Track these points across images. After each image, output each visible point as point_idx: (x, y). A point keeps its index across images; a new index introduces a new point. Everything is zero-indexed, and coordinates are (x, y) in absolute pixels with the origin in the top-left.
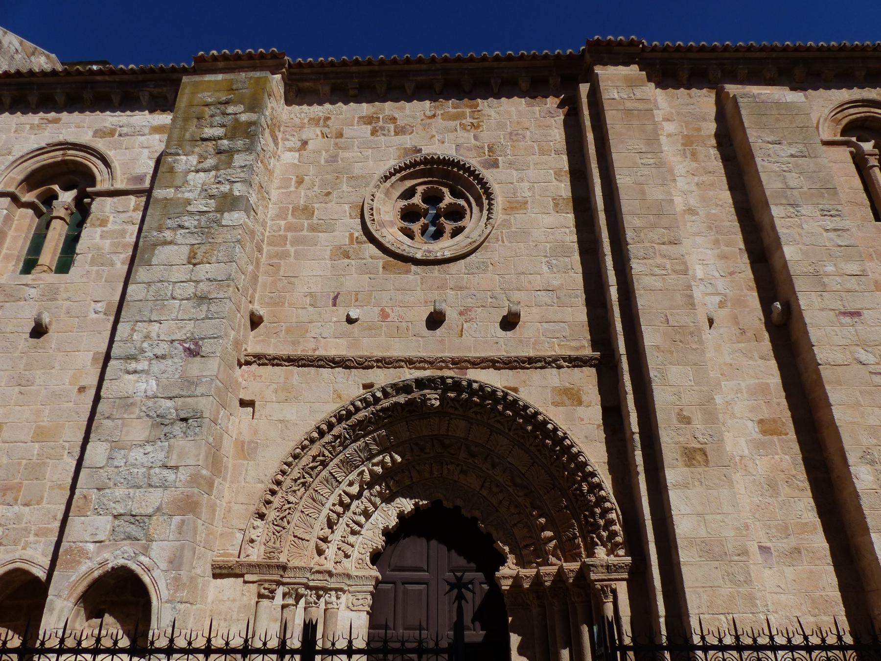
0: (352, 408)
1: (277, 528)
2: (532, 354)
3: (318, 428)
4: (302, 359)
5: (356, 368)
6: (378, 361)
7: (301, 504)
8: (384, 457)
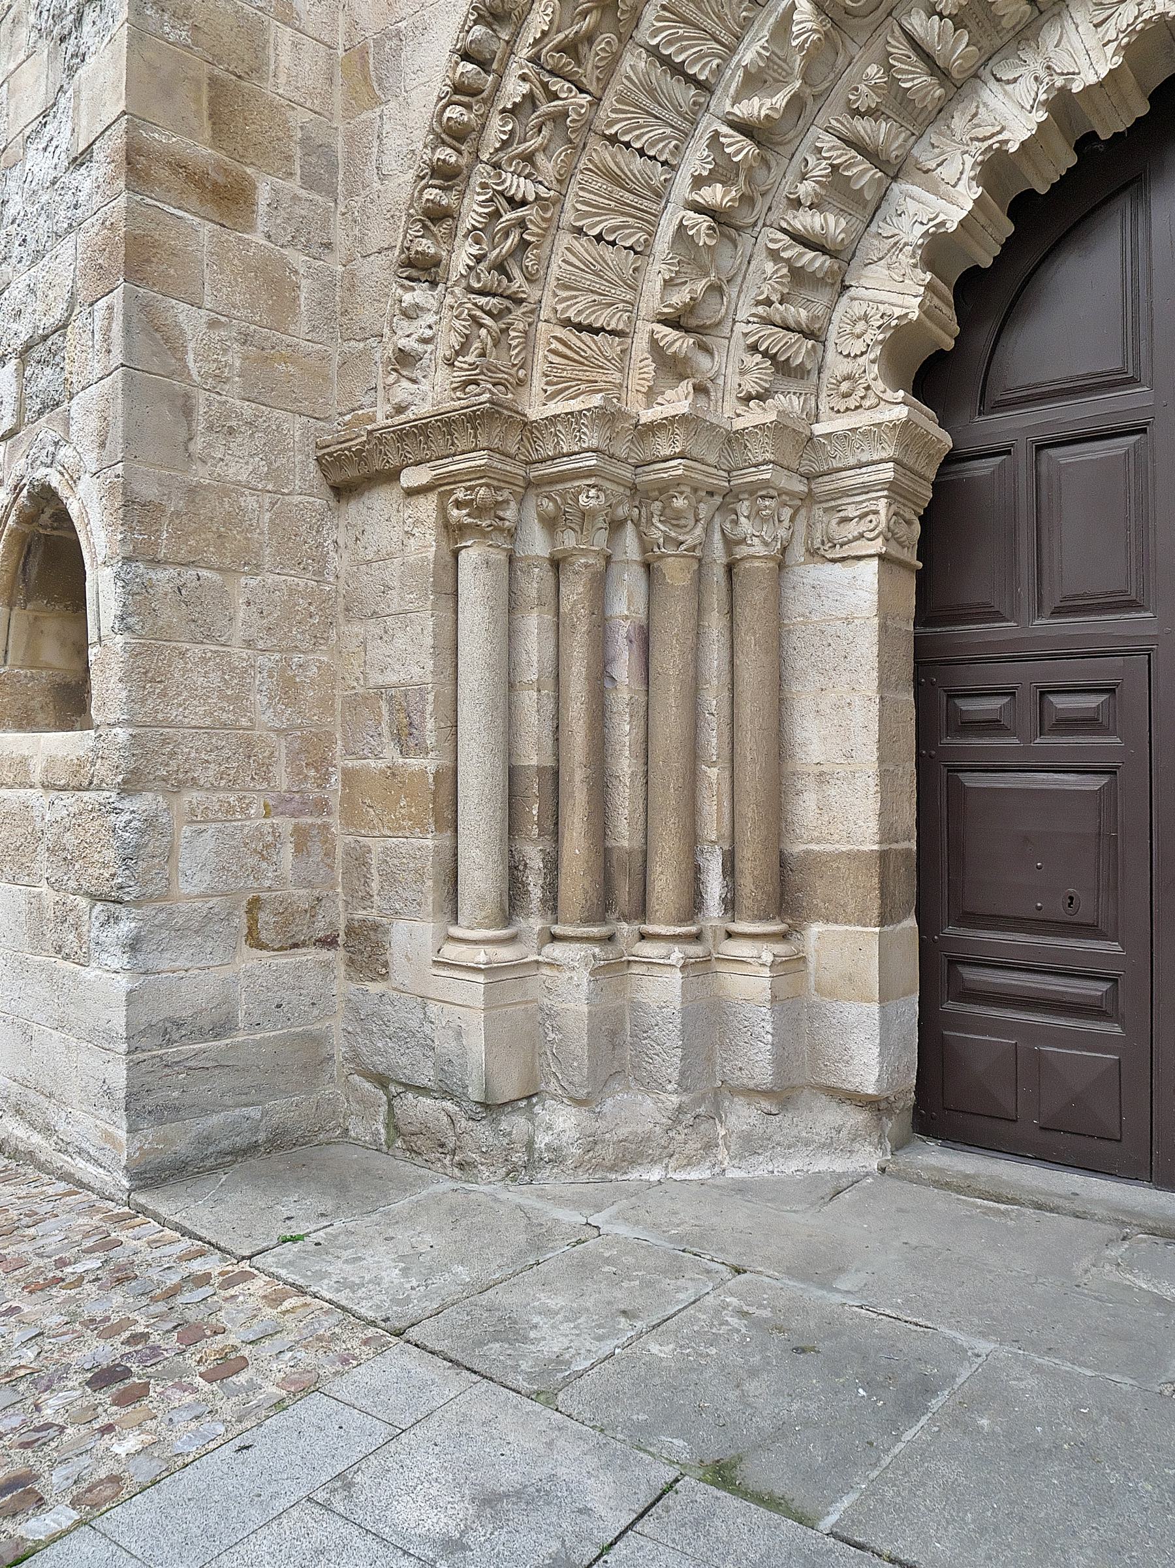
1: (482, 300)
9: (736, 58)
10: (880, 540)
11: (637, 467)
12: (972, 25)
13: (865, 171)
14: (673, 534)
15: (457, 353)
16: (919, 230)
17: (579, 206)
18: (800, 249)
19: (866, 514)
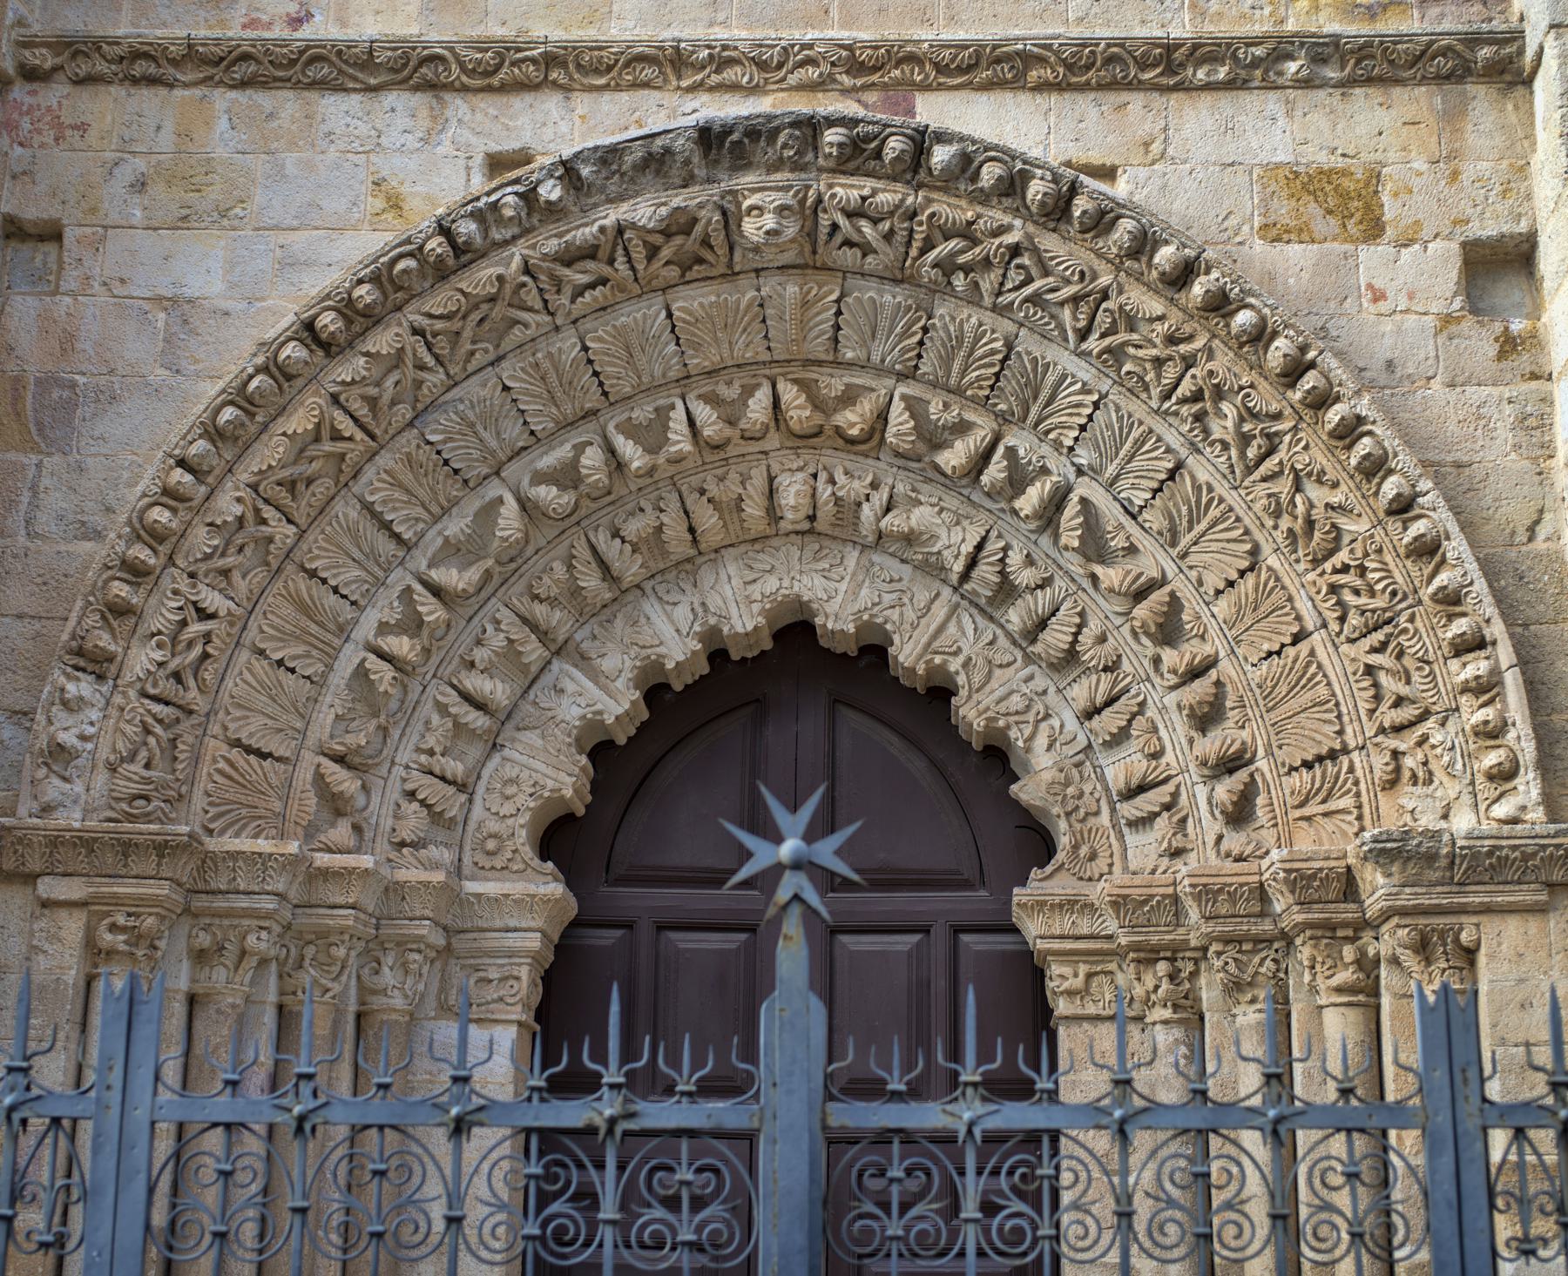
0: (436, 245)
1: (157, 708)
2: (1181, 28)
3: (309, 326)
4: (246, 57)
5: (465, 89)
6: (551, 60)
7: (253, 625)
8: (579, 449)
9: (439, 526)
10: (519, 1008)
11: (296, 906)
12: (644, 549)
13: (534, 650)
14: (324, 981)
15: (122, 760)
16: (576, 712)
17: (265, 628)
18: (466, 707)
19: (506, 978)
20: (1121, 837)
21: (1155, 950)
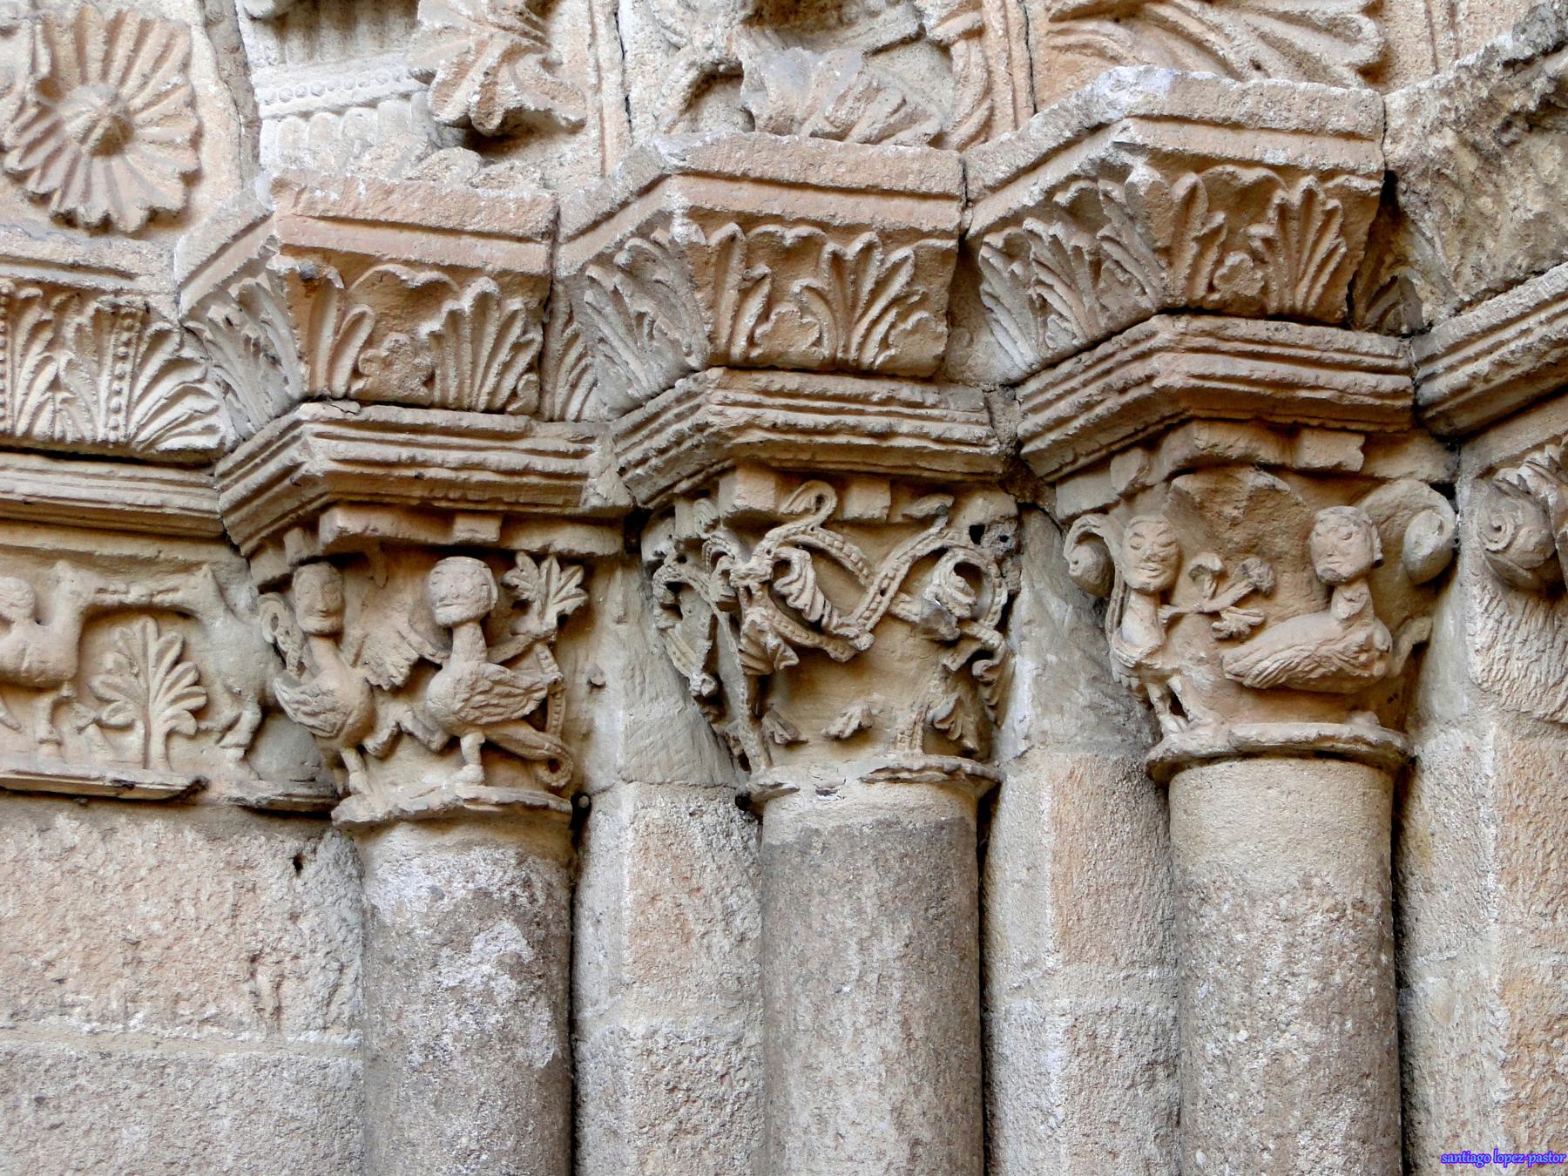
20: (235, 66)
21: (435, 508)
